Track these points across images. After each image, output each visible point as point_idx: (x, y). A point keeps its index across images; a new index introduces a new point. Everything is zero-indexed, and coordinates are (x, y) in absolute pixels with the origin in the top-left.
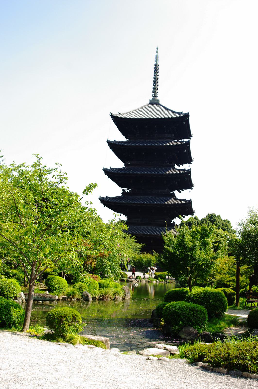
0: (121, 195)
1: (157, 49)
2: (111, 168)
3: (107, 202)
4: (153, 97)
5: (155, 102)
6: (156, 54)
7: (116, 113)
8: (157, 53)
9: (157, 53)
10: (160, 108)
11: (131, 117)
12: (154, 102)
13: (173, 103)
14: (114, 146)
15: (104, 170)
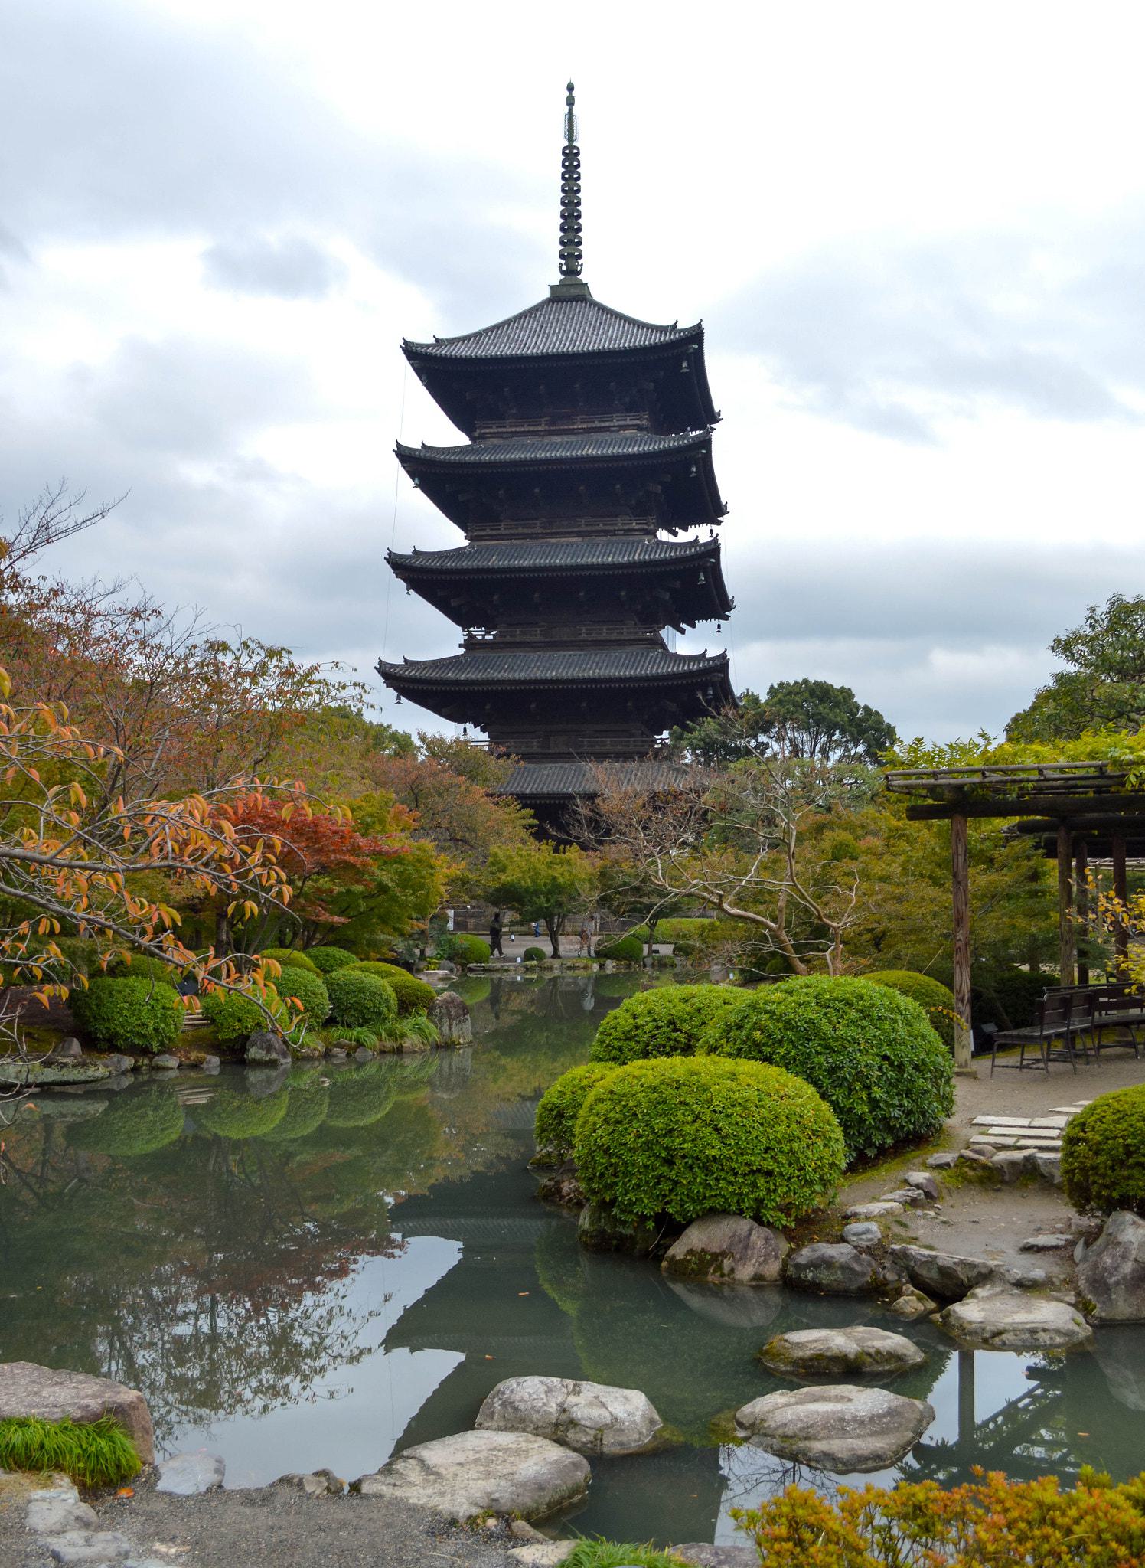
0: (462, 651)
1: (570, 88)
2: (415, 552)
3: (411, 683)
4: (562, 272)
5: (573, 291)
6: (567, 109)
7: (423, 337)
8: (570, 102)
9: (570, 102)
10: (592, 313)
11: (481, 353)
12: (570, 293)
13: (640, 286)
14: (424, 467)
15: (388, 560)
